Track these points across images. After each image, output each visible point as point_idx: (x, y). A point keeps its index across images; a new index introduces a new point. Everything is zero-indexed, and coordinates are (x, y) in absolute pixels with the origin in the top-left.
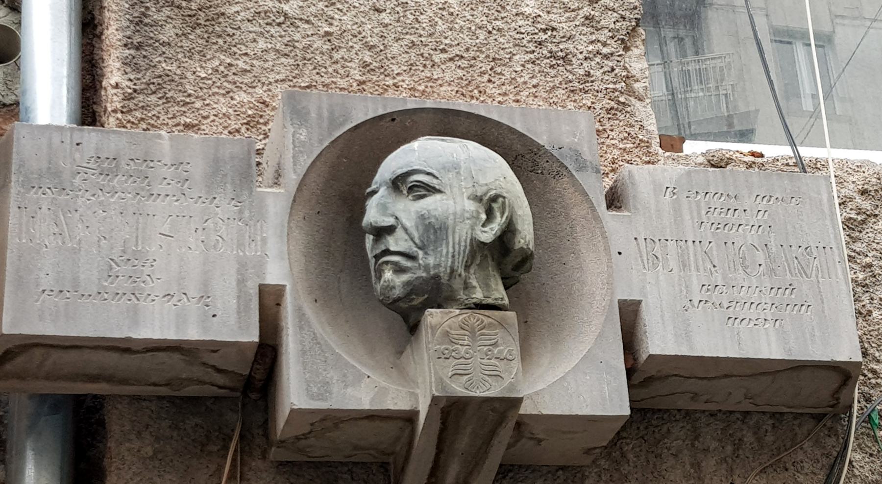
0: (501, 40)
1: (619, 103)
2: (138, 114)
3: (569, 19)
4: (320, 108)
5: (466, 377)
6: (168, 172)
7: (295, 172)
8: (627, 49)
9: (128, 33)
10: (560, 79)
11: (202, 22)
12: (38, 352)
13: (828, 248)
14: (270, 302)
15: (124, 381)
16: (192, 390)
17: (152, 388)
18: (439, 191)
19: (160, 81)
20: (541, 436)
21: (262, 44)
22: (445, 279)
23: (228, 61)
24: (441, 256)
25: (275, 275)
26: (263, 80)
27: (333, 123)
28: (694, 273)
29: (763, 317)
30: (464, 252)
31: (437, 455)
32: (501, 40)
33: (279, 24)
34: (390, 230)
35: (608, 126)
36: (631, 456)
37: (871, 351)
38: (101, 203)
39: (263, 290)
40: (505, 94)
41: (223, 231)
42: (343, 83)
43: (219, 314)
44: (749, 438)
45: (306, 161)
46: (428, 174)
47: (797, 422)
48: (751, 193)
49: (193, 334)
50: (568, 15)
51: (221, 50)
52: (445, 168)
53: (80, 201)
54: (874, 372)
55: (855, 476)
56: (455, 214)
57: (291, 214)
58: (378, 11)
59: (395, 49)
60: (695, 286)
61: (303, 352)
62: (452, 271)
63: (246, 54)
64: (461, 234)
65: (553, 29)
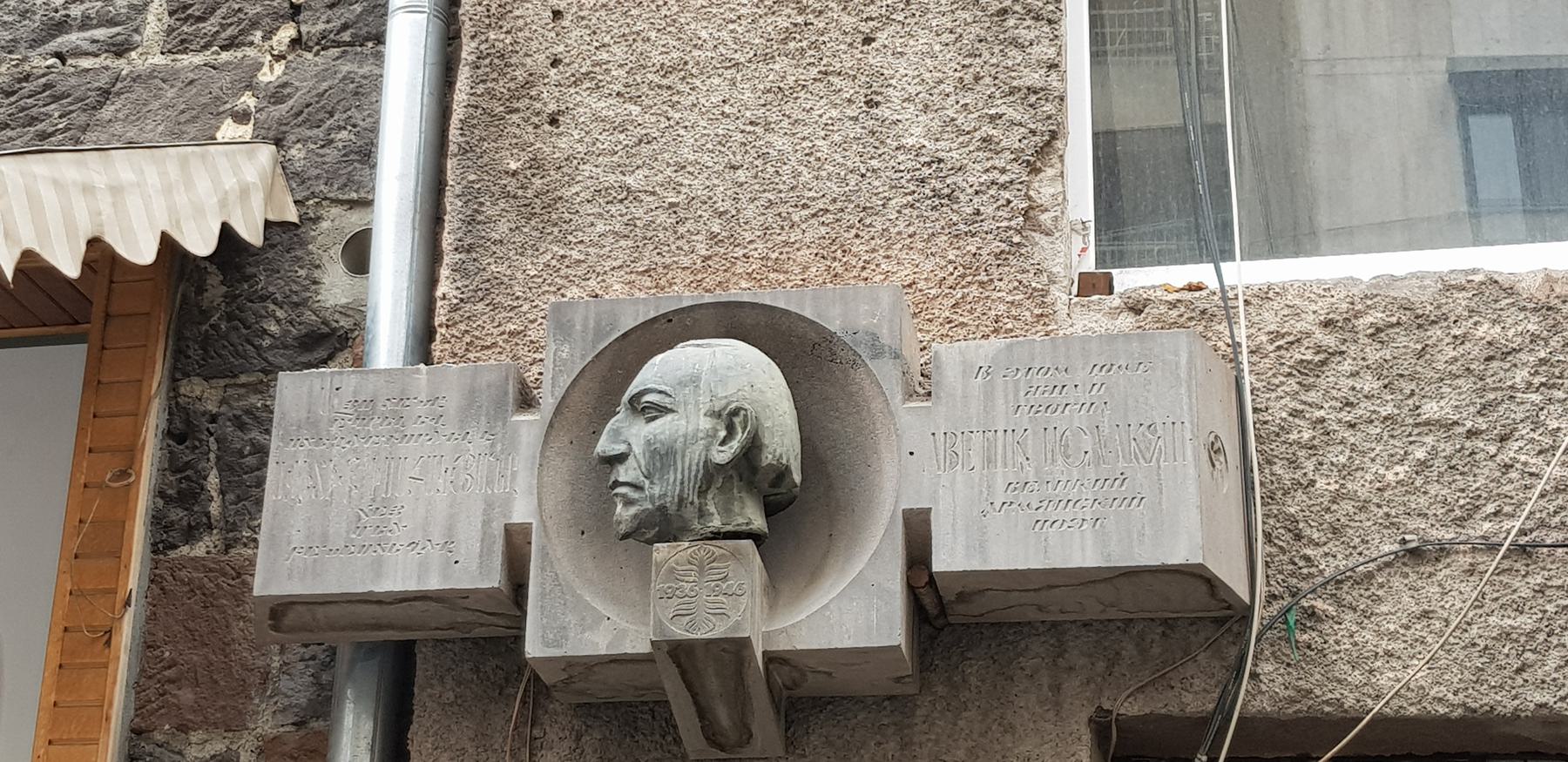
0: (876, 183)
1: (1012, 244)
2: (463, 327)
3: (963, 145)
4: (586, 318)
6: (421, 409)
8: (1035, 171)
10: (943, 223)
11: (538, 210)
13: (1178, 425)
14: (518, 540)
18: (672, 411)
19: (487, 285)
22: (672, 509)
23: (562, 252)
25: (522, 512)
26: (598, 269)
27: (599, 334)
28: (1000, 469)
29: (1080, 516)
31: (694, 696)
32: (876, 183)
33: (621, 201)
34: (621, 458)
35: (996, 276)
36: (973, 680)
37: (1308, 532)
38: (355, 450)
39: (509, 531)
40: (874, 251)
42: (686, 262)
43: (461, 560)
44: (1129, 650)
45: (565, 381)
47: (1194, 628)
48: (1086, 363)
49: (434, 584)
50: (961, 139)
51: (557, 241)
52: (682, 384)
53: (335, 450)
54: (1307, 559)
55: (1261, 692)
56: (685, 436)
58: (734, 168)
59: (750, 211)
60: (1000, 484)
61: (543, 595)
62: (681, 500)
64: (694, 456)
65: (940, 161)
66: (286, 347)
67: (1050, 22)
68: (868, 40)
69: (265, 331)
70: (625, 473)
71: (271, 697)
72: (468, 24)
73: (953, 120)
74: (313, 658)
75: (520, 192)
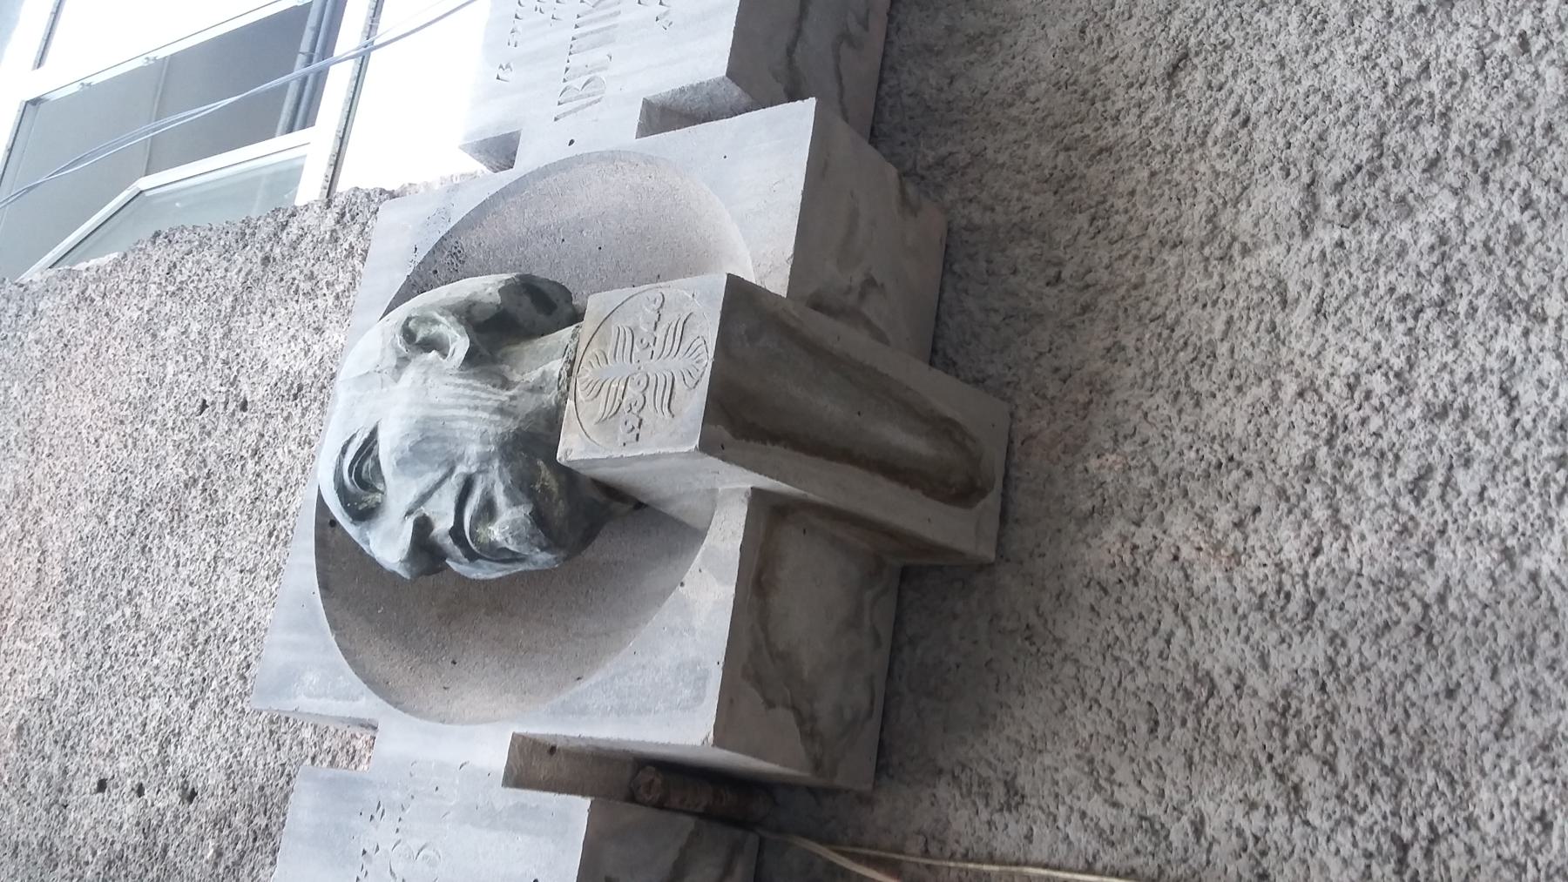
5: (678, 385)
14: (543, 769)
18: (374, 433)
20: (857, 278)
22: (511, 424)
24: (468, 430)
25: (494, 754)
30: (475, 388)
41: (415, 843)
46: (344, 451)
61: (621, 711)
67: (293, 215)
70: (443, 525)
73: (337, 297)
75: (239, 846)
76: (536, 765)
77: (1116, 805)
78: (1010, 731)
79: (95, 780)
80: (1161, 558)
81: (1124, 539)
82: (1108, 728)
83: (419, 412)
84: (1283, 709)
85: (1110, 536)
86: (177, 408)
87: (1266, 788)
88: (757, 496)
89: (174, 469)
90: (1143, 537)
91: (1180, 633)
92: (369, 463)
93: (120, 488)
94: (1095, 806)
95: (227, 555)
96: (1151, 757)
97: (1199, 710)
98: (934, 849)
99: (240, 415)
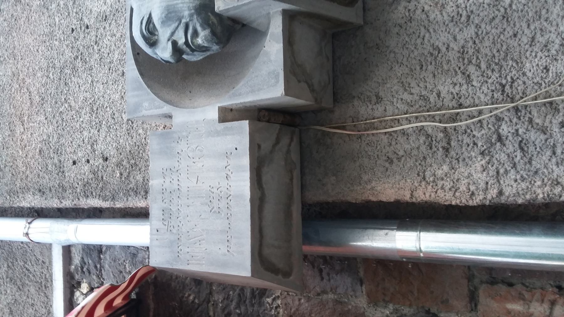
6: (168, 180)
7: (162, 107)
9: (141, 197)
12: (266, 251)
15: (290, 197)
16: (295, 156)
17: (295, 181)
18: (150, 15)
21: (141, 131)
24: (183, 7)
25: (213, 114)
41: (194, 146)
45: (158, 101)
46: (141, 23)
49: (246, 161)
57: (183, 108)
61: (253, 91)
63: (145, 139)
66: (199, 292)
68: (87, 27)
69: (193, 302)
70: (181, 41)
71: (349, 299)
72: (75, 202)
74: (328, 274)
75: (127, 171)
76: (228, 115)
77: (412, 94)
78: (375, 79)
79: (71, 161)
80: (419, 12)
81: (406, 8)
82: (407, 71)
83: (164, 4)
84: (463, 52)
85: (401, 8)
86: (63, 33)
87: (460, 78)
88: (285, 13)
89: (68, 54)
90: (411, 6)
91: (427, 35)
92: (151, 25)
93: (51, 65)
94: (406, 96)
95: (96, 80)
96: (422, 77)
97: (435, 58)
98: (355, 120)
99: (87, 31)
